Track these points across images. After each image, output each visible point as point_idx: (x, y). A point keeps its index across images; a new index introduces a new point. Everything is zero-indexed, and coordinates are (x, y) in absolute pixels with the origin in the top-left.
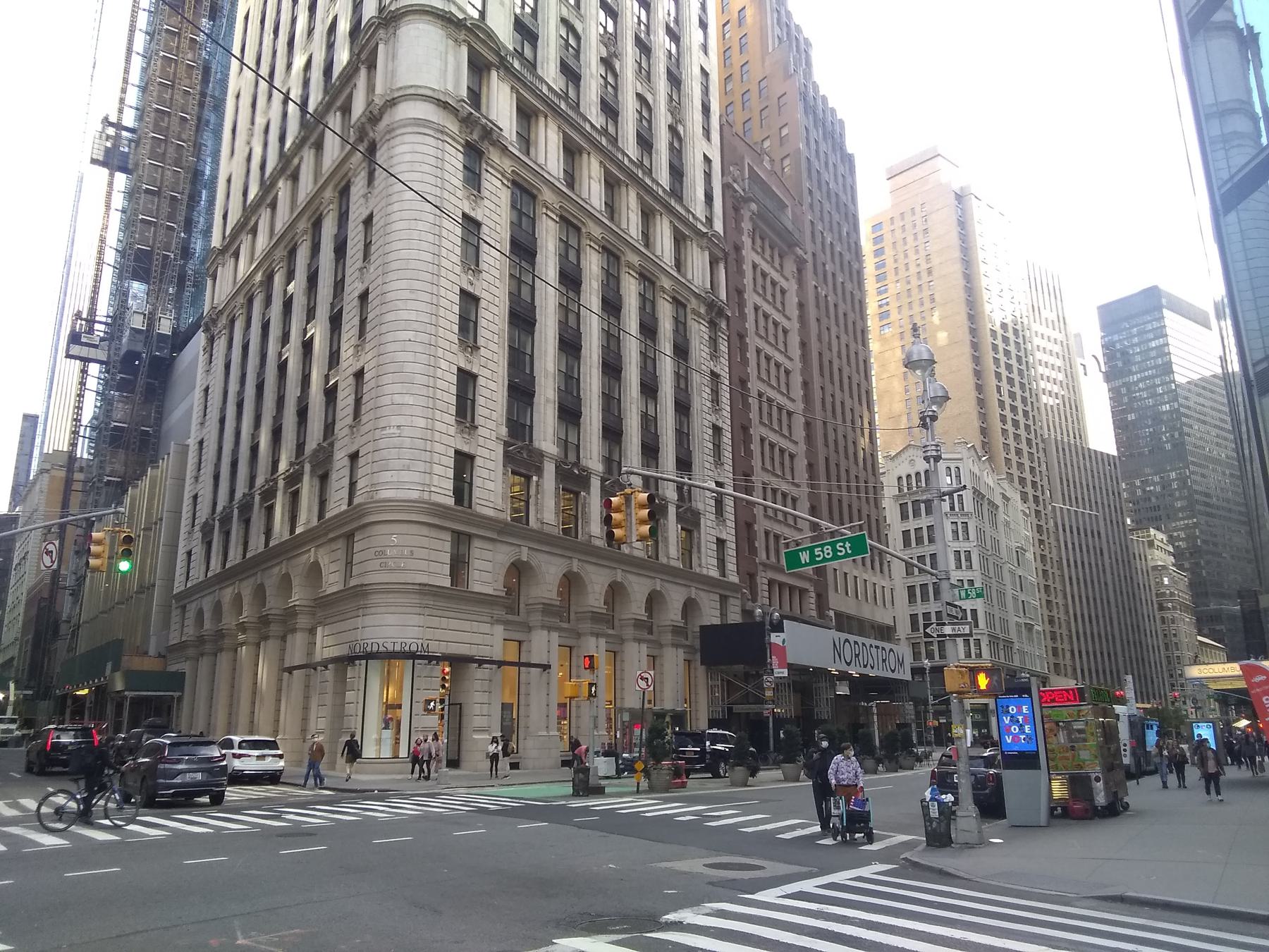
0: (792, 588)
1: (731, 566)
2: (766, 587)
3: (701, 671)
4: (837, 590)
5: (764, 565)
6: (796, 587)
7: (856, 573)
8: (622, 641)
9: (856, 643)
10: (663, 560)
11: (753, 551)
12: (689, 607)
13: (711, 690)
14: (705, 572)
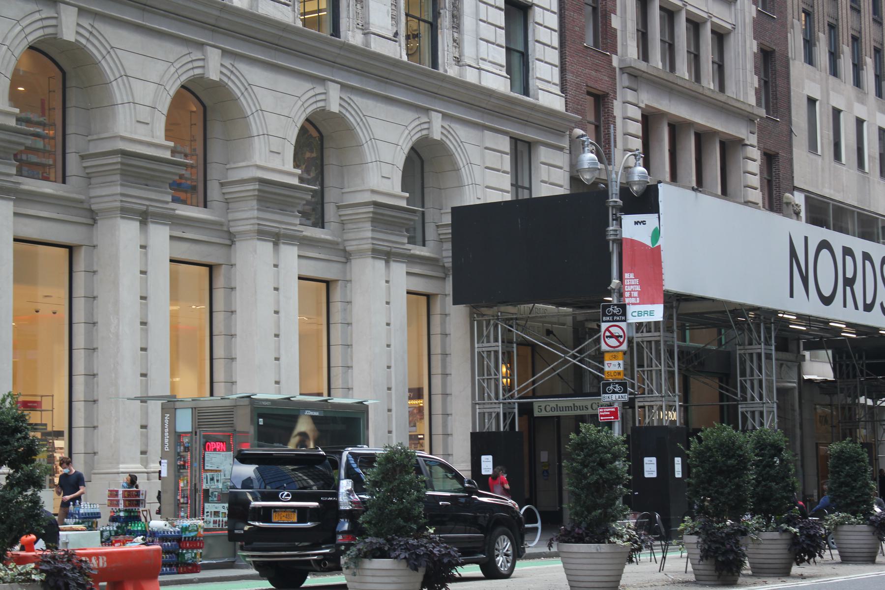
0: (702, 137)
1: (545, 69)
2: (636, 128)
3: (456, 318)
4: (813, 147)
5: (635, 76)
6: (713, 133)
7: (860, 111)
8: (231, 239)
9: (847, 252)
10: (352, 36)
11: (606, 38)
12: (424, 164)
13: (482, 367)
14: (471, 76)
